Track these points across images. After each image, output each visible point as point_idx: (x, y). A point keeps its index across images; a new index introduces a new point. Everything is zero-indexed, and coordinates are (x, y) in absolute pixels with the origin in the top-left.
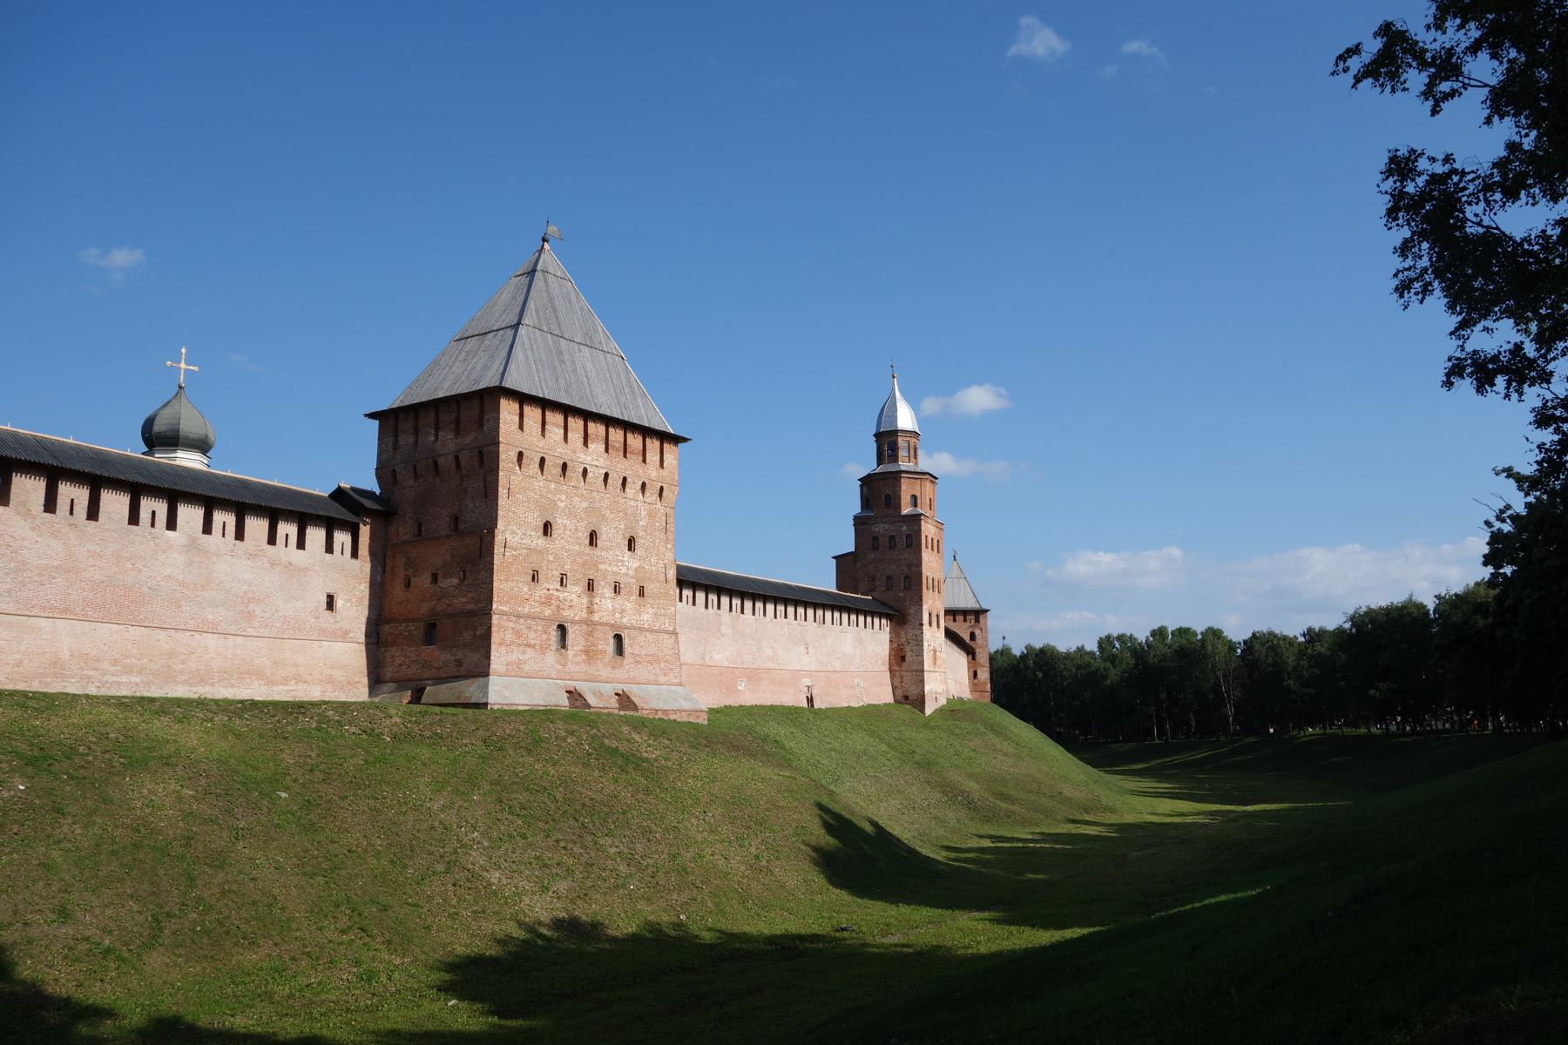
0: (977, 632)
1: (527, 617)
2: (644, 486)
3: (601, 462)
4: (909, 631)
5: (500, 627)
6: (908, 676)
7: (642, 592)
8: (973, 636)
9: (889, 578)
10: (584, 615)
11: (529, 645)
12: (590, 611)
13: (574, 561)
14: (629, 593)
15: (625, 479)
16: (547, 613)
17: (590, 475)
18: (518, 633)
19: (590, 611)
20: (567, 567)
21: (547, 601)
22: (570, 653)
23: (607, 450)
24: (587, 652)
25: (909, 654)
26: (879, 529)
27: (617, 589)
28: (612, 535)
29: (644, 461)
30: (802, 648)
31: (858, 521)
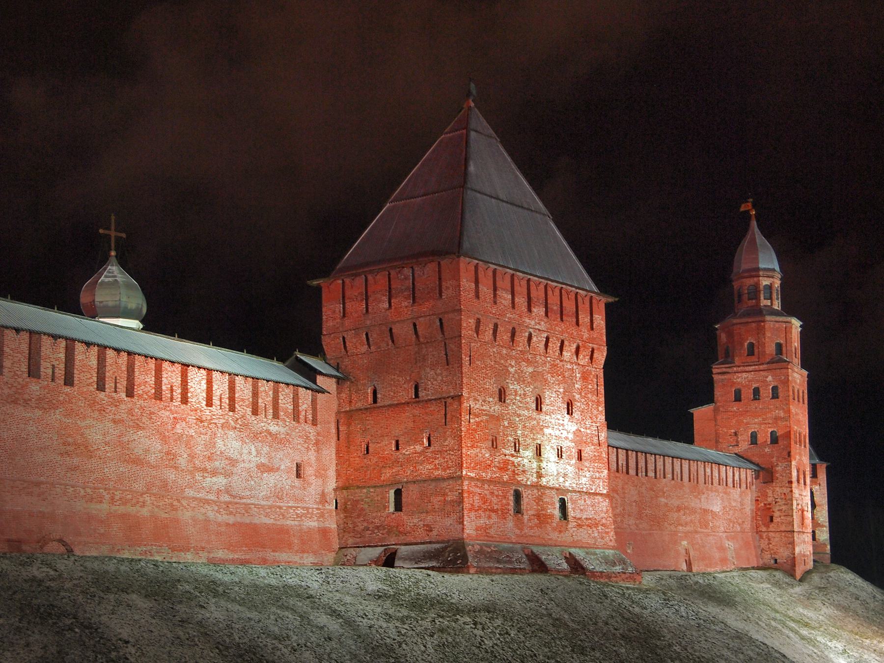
3: (543, 326)
4: (775, 492)
6: (776, 538)
10: (535, 480)
11: (493, 510)
14: (570, 457)
16: (506, 478)
17: (534, 339)
22: (526, 517)
24: (538, 516)
25: (777, 514)
29: (577, 324)
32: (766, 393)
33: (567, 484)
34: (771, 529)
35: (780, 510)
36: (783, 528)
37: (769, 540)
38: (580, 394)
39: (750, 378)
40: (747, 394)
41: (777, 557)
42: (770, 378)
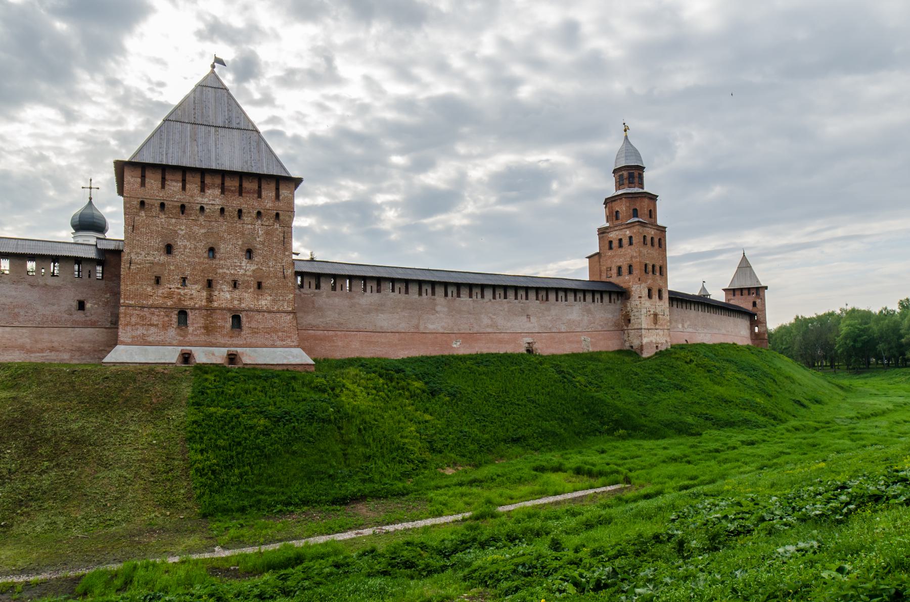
0: (758, 301)
1: (150, 307)
2: (259, 213)
3: (218, 201)
5: (126, 314)
7: (259, 285)
8: (754, 304)
10: (204, 303)
12: (210, 299)
13: (194, 269)
15: (240, 211)
18: (143, 318)
19: (210, 299)
20: (187, 273)
21: (170, 296)
22: (190, 329)
23: (223, 192)
24: (206, 328)
25: (632, 318)
27: (235, 285)
28: (229, 247)
29: (260, 196)
30: (524, 318)
33: (243, 305)
36: (636, 327)
38: (263, 244)
40: (615, 244)
42: (628, 232)
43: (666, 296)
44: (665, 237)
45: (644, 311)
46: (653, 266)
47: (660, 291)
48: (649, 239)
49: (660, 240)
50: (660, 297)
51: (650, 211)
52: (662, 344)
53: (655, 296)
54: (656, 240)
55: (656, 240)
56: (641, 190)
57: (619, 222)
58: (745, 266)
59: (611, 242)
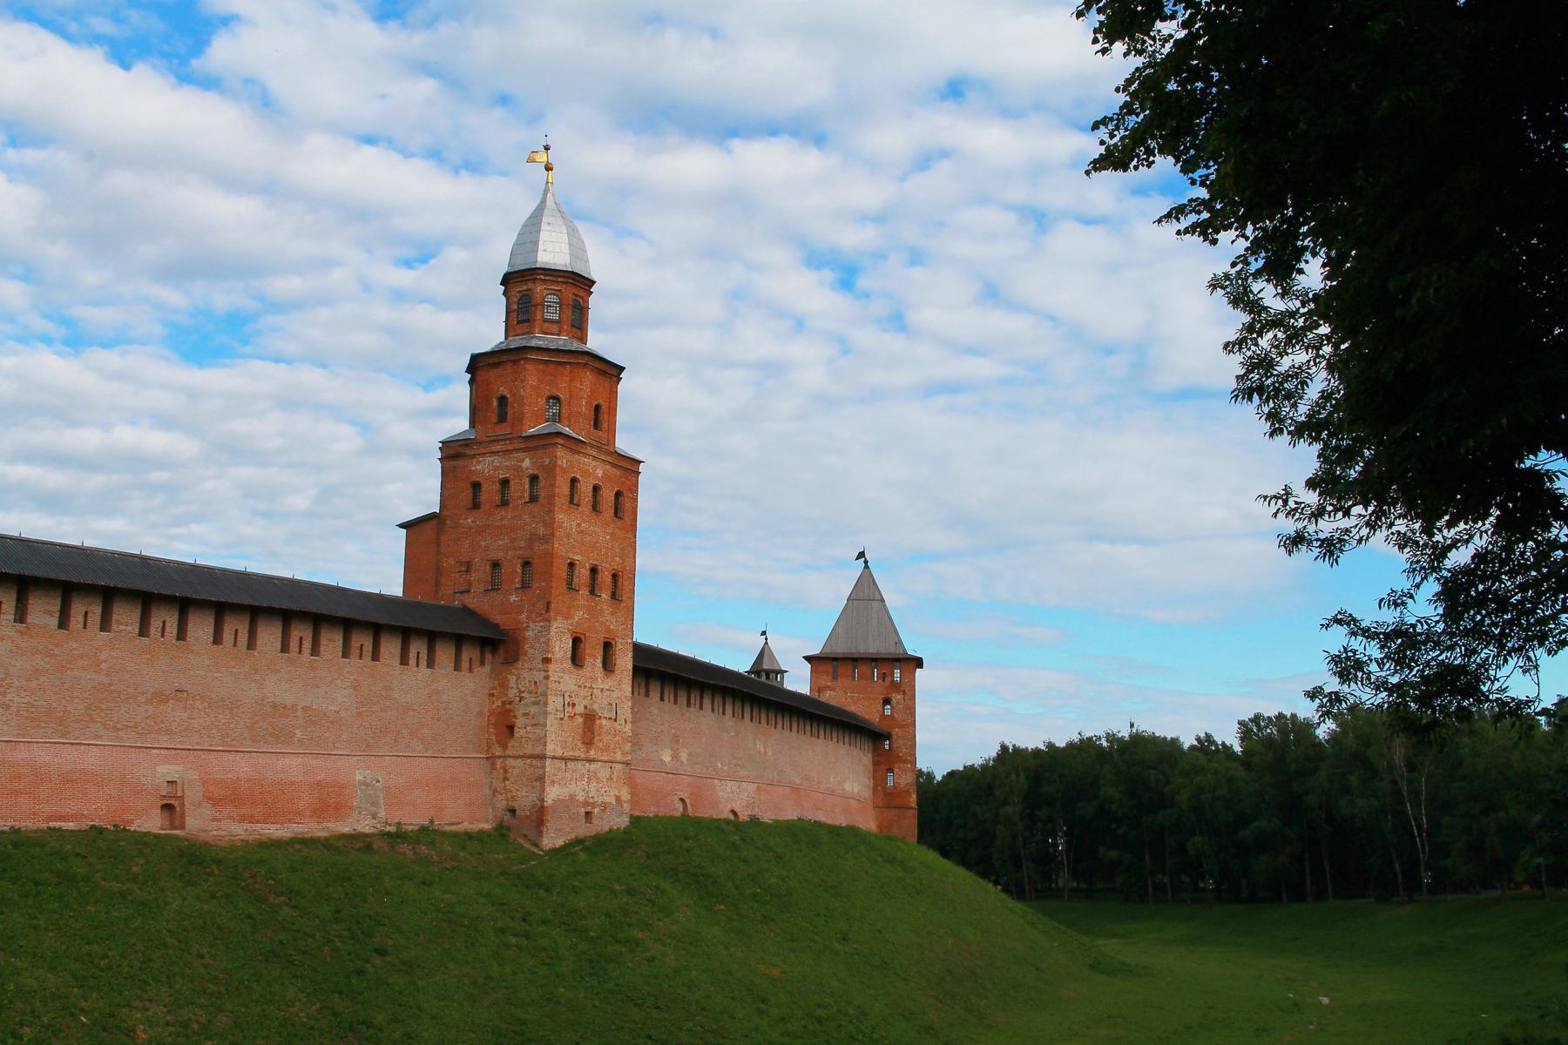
9: (496, 565)
25: (520, 721)
26: (485, 466)
31: (453, 452)
32: (520, 489)
34: (510, 752)
35: (526, 714)
36: (529, 750)
37: (506, 771)
39: (496, 464)
40: (490, 492)
41: (515, 805)
42: (527, 463)
43: (625, 662)
44: (634, 488)
45: (554, 703)
46: (594, 570)
47: (607, 646)
48: (585, 489)
49: (618, 494)
50: (608, 665)
51: (597, 408)
52: (605, 806)
53: (594, 662)
54: (608, 496)
55: (608, 496)
56: (575, 345)
57: (505, 429)
58: (865, 595)
59: (476, 486)
